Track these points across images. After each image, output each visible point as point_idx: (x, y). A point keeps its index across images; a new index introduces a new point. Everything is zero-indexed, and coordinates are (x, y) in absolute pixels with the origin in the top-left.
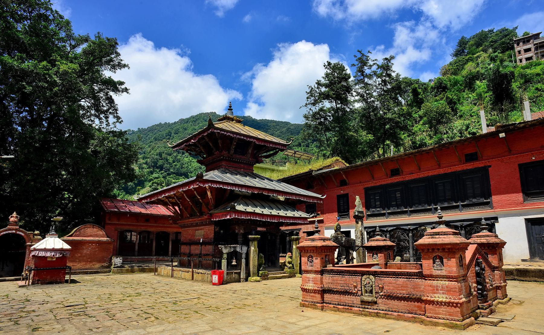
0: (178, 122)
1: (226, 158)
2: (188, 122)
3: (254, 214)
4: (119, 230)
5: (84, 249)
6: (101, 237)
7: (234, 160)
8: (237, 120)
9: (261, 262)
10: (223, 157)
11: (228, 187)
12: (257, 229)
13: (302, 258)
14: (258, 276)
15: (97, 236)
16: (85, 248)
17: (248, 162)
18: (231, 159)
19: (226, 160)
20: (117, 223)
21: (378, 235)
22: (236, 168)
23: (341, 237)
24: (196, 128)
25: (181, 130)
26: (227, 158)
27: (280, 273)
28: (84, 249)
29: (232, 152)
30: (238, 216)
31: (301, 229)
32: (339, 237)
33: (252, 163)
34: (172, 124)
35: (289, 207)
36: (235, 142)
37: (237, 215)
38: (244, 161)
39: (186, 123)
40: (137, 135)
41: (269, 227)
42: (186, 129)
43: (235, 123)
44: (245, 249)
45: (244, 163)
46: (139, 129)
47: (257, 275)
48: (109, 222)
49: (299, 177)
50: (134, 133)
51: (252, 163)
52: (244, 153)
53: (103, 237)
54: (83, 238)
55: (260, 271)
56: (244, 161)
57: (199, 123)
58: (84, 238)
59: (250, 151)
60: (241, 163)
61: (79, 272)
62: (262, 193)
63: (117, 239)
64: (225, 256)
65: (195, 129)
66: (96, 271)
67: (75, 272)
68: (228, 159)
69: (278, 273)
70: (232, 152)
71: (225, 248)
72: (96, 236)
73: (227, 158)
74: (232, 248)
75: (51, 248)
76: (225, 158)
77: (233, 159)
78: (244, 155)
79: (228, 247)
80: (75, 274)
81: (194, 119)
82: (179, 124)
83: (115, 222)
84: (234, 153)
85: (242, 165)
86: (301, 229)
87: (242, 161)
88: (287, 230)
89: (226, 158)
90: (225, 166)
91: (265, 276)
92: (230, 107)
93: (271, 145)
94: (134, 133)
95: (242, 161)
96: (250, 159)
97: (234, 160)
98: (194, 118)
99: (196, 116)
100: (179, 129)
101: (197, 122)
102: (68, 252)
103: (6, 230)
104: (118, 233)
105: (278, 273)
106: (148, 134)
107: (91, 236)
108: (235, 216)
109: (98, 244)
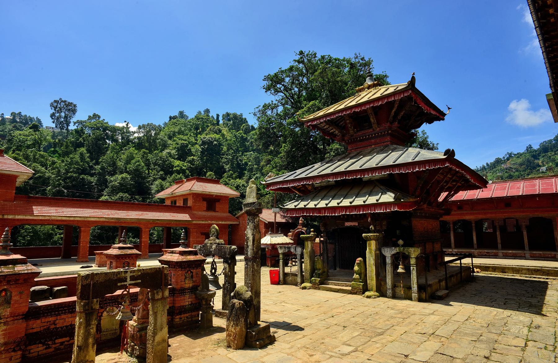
1: (348, 141)
12: (344, 224)
23: (211, 244)
27: (344, 285)
32: (208, 245)
41: (362, 221)
44: (299, 250)
45: (375, 137)
60: (372, 138)
64: (281, 256)
68: (351, 140)
74: (287, 249)
75: (281, 243)
85: (373, 141)
87: (369, 136)
89: (348, 141)
90: (351, 150)
91: (315, 285)
95: (369, 136)
103: (297, 230)
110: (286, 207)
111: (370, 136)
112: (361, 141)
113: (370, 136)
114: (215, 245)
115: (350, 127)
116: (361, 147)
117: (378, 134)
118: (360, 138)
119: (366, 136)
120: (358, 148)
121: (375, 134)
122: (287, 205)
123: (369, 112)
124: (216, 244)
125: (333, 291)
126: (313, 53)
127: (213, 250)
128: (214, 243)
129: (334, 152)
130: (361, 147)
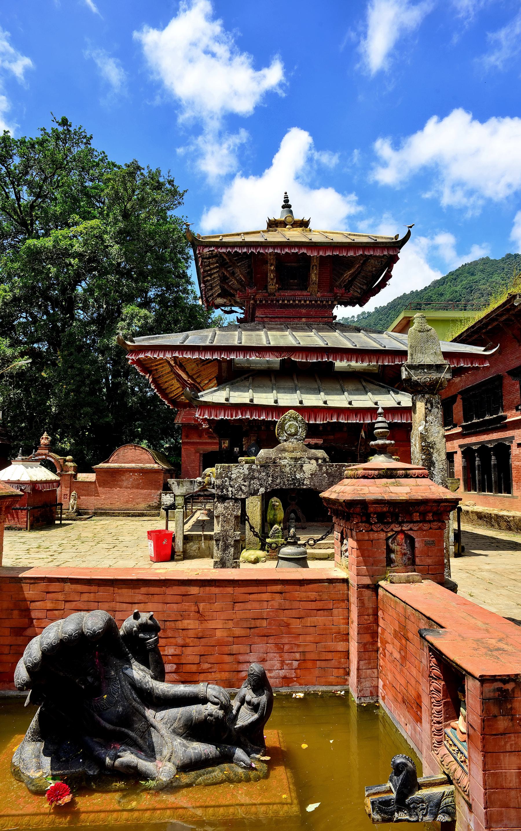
0: (429, 286)
1: (261, 301)
2: (444, 283)
3: (251, 407)
4: (202, 452)
5: (123, 480)
6: (146, 463)
7: (280, 302)
8: (294, 223)
9: (271, 517)
10: (256, 302)
11: (193, 354)
13: (169, 522)
14: (262, 549)
15: (140, 461)
16: (124, 478)
17: (316, 301)
18: (272, 301)
19: (261, 306)
20: (198, 441)
21: (382, 450)
22: (290, 318)
23: (296, 459)
24: (457, 290)
25: (434, 297)
26: (264, 302)
28: (123, 480)
29: (272, 287)
30: (210, 416)
31: (513, 438)
33: (327, 302)
34: (422, 291)
35: (380, 386)
36: (271, 265)
37: (207, 412)
38: (305, 301)
39: (442, 285)
40: (374, 317)
41: (332, 437)
42: (442, 295)
43: (289, 229)
46: (376, 308)
47: (259, 546)
48: (186, 440)
49: (493, 320)
50: (370, 316)
51: (327, 302)
52: (304, 284)
53: (150, 463)
54: (120, 465)
55: (268, 537)
56: (305, 301)
57: (462, 281)
58: (123, 465)
59: (314, 277)
60: (302, 306)
61: (119, 513)
62: (289, 359)
63: (200, 466)
65: (456, 292)
66: (141, 513)
67: (113, 513)
69: (326, 546)
70: (272, 287)
71: (178, 485)
72: (139, 462)
73: (264, 302)
76: (258, 302)
77: (278, 301)
78: (306, 290)
79: (185, 481)
80: (114, 516)
81: (454, 277)
82: (432, 288)
83: (195, 441)
84: (279, 289)
85: (304, 311)
86: (513, 438)
87: (300, 301)
88: (490, 442)
89: (261, 301)
92: (286, 201)
93: (351, 254)
94: (370, 316)
95: (300, 301)
96: (319, 294)
97: (280, 302)
98: (453, 275)
99: (456, 271)
100: (431, 297)
101: (459, 280)
102: (27, 485)
104: (200, 457)
105: (326, 546)
106: (390, 314)
107: (132, 462)
108: (210, 416)
109: (142, 473)
110: (201, 399)
111: (303, 302)
112: (283, 306)
113: (303, 302)
114: (313, 462)
115: (272, 279)
116: (282, 317)
117: (316, 301)
118: (283, 301)
119: (294, 301)
120: (277, 317)
121: (311, 301)
122: (202, 396)
123: (315, 262)
124: (317, 459)
125: (317, 559)
126: (83, 134)
127: (307, 475)
128: (310, 459)
129: (139, 321)
130: (282, 317)
